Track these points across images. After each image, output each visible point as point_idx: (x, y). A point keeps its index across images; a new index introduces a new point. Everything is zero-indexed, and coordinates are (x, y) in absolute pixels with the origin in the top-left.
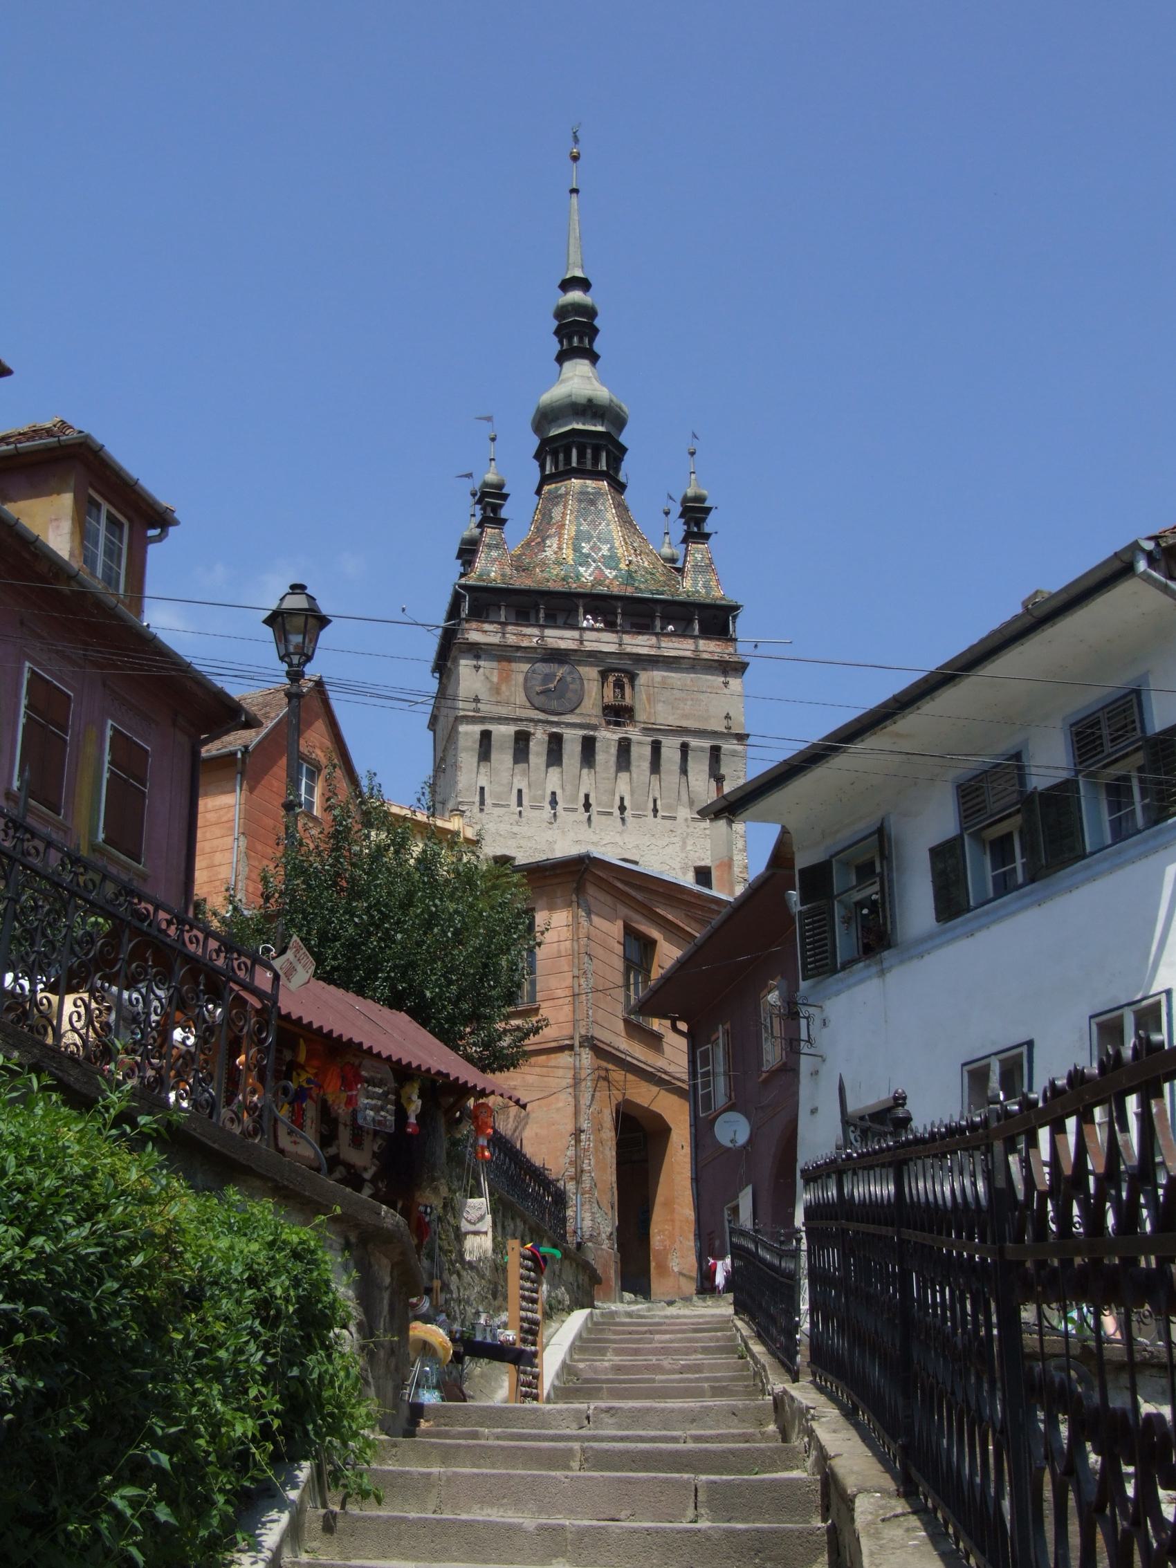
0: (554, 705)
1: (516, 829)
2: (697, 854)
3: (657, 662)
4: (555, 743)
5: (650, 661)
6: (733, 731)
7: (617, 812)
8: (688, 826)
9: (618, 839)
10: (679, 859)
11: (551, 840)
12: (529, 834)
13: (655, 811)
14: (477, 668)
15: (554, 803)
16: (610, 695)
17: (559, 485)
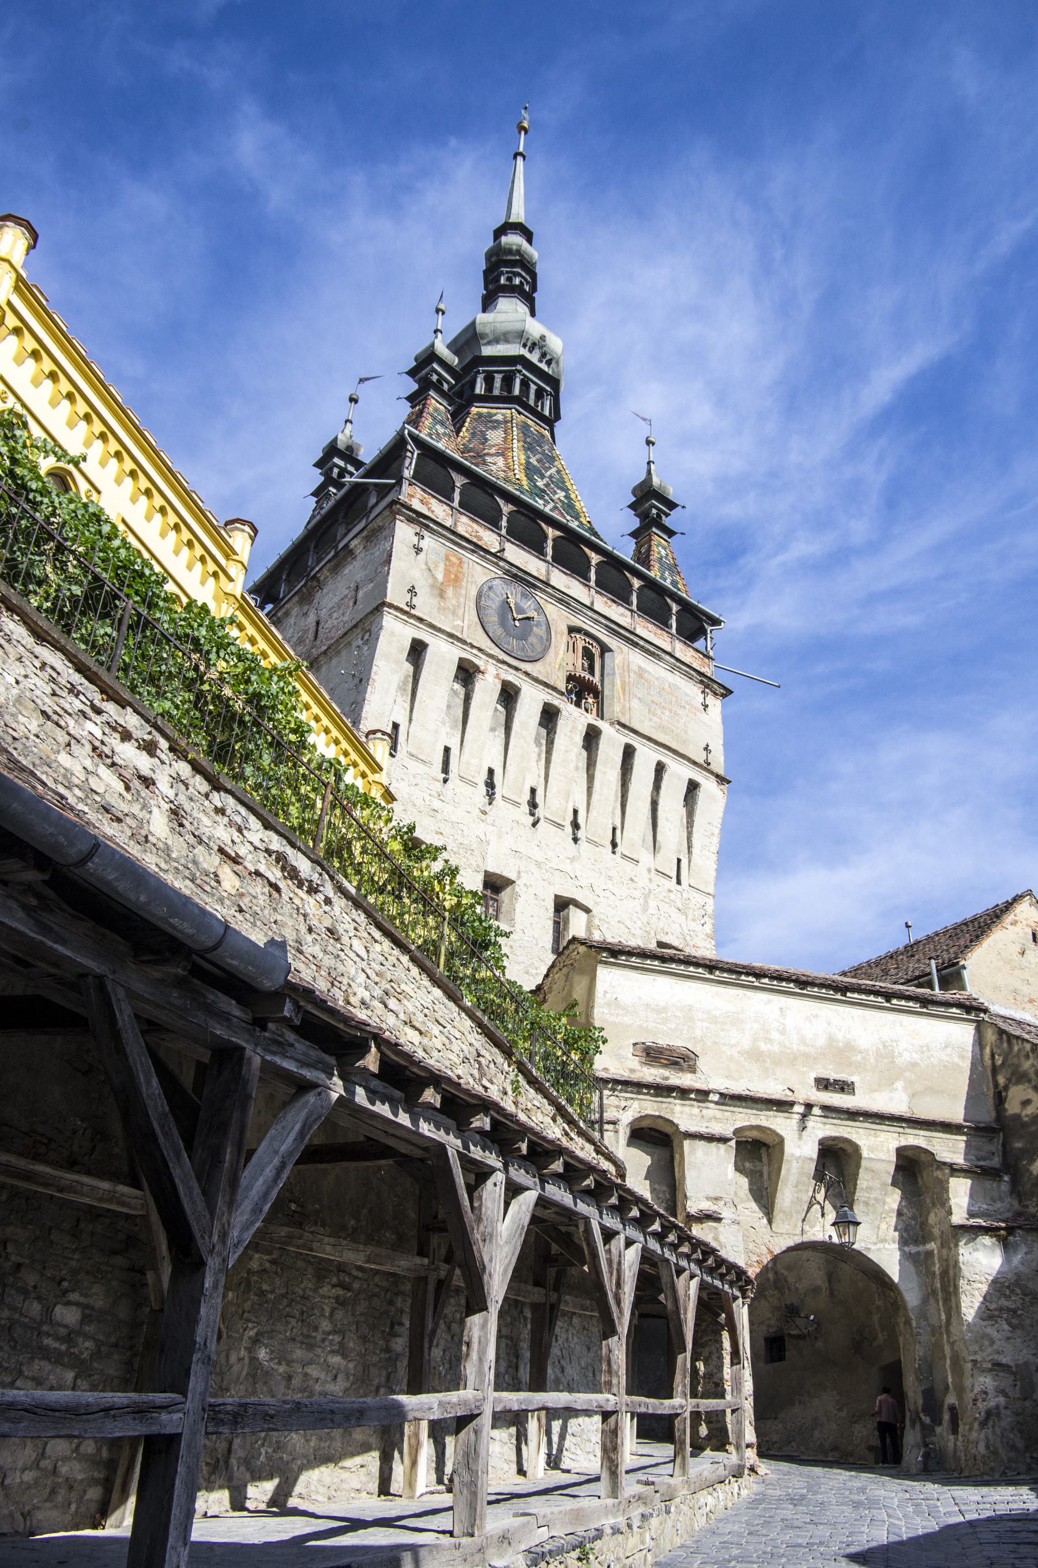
0: (514, 644)
1: (436, 804)
2: (661, 925)
3: (635, 645)
4: (509, 696)
5: (627, 640)
6: (711, 767)
7: (569, 829)
8: (650, 880)
9: (567, 867)
10: (639, 923)
11: (483, 838)
12: (454, 818)
13: (614, 845)
14: (418, 550)
15: (490, 785)
16: (577, 664)
17: (494, 411)
